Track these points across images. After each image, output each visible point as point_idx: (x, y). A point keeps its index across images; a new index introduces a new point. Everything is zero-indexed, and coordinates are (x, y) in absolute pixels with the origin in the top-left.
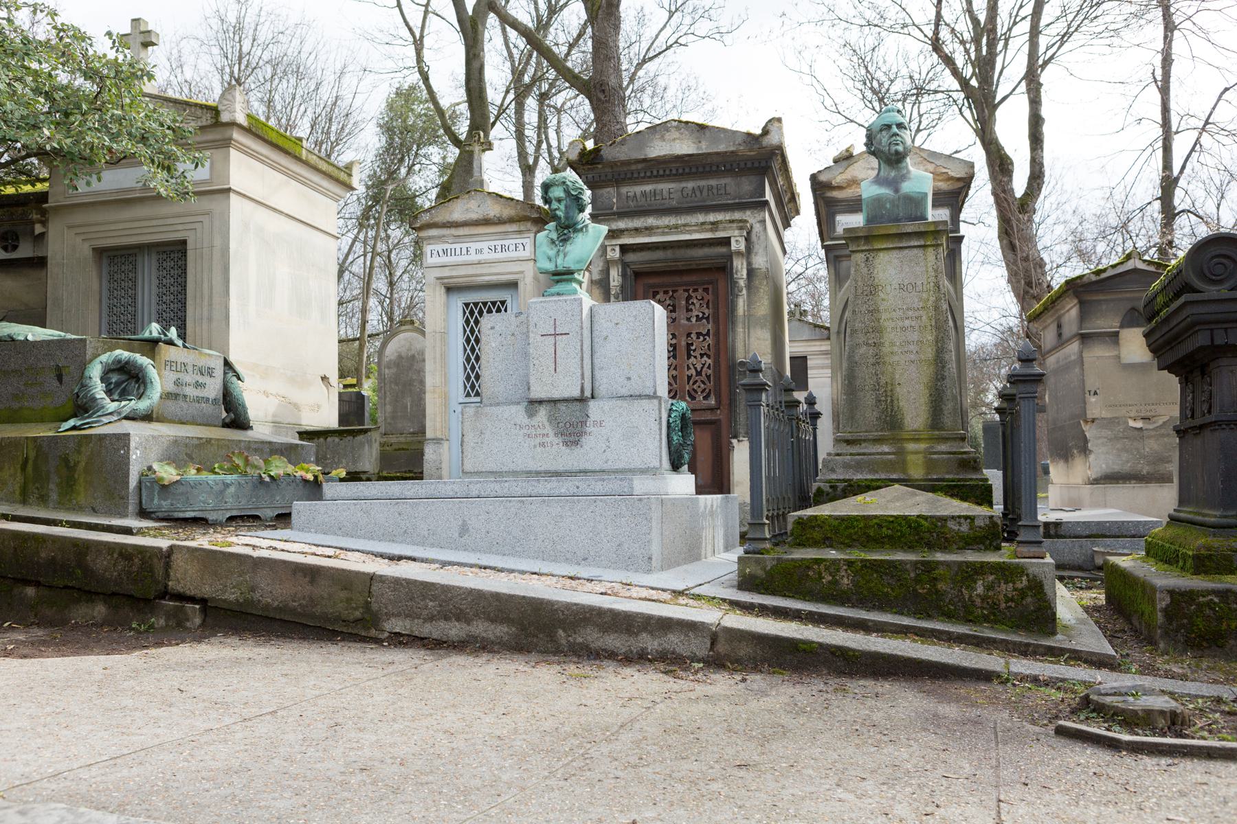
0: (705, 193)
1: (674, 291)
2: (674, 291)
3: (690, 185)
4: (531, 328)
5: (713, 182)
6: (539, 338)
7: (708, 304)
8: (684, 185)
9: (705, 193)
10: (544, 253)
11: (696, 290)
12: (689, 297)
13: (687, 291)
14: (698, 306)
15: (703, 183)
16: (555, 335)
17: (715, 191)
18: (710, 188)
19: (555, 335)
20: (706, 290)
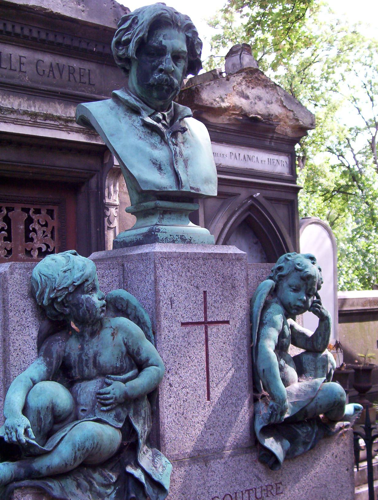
0: (65, 74)
1: (9, 209)
2: (9, 209)
3: (47, 59)
4: (164, 308)
5: (75, 64)
6: (177, 329)
7: (52, 233)
8: (39, 56)
9: (65, 74)
10: (138, 150)
11: (37, 211)
12: (29, 221)
13: (27, 210)
14: (40, 233)
15: (63, 61)
16: (206, 323)
17: (77, 77)
18: (72, 71)
19: (206, 323)
20: (50, 213)
